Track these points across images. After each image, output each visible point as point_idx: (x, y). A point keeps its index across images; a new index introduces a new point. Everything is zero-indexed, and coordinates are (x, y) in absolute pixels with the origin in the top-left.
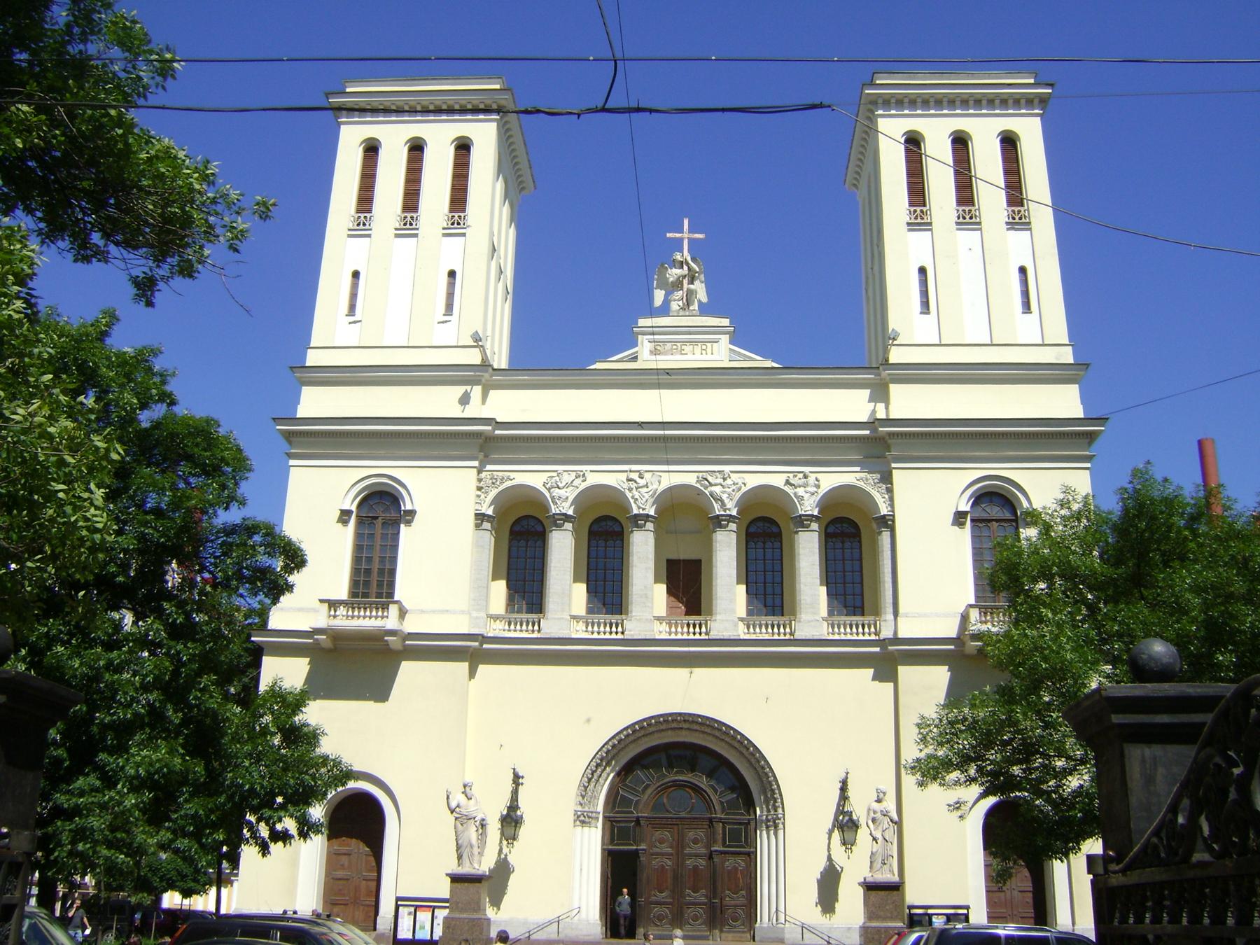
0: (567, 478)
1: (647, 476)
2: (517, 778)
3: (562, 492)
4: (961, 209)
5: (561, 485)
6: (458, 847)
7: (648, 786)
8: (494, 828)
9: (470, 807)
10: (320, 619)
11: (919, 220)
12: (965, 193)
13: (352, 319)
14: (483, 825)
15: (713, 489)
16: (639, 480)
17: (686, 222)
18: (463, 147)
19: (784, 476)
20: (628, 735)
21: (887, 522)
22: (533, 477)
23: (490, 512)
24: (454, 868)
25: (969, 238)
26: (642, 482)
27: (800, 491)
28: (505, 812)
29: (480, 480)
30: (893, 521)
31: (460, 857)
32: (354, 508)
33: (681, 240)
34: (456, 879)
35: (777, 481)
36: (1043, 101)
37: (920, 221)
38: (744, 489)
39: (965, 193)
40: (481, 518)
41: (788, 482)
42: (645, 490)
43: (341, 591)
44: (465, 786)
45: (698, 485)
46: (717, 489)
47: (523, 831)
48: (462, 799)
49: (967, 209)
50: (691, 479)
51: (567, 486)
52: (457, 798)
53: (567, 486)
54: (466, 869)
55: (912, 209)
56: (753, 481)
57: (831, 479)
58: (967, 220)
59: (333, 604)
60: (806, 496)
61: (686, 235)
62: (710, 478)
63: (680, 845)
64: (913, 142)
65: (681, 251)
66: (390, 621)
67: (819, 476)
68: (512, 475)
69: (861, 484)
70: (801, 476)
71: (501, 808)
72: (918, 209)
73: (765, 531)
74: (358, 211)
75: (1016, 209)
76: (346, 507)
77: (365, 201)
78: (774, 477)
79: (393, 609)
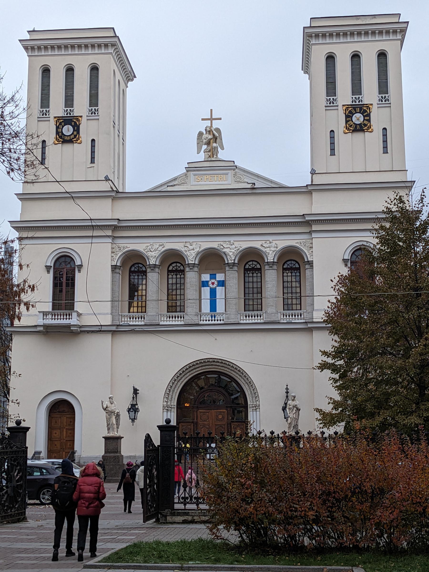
0: (156, 246)
2: (136, 391)
3: (153, 254)
4: (354, 97)
5: (152, 249)
6: (108, 425)
8: (125, 417)
9: (112, 408)
10: (40, 321)
14: (118, 416)
16: (190, 247)
19: (260, 243)
20: (187, 369)
21: (310, 263)
22: (139, 246)
23: (118, 264)
24: (106, 434)
26: (191, 247)
27: (268, 250)
28: (130, 407)
29: (112, 248)
31: (108, 429)
32: (52, 265)
34: (106, 438)
35: (257, 245)
38: (241, 249)
40: (114, 268)
43: (48, 307)
44: (110, 398)
47: (139, 415)
48: (109, 405)
50: (215, 245)
51: (155, 250)
52: (107, 403)
53: (155, 250)
54: (111, 434)
55: (328, 98)
56: (245, 245)
59: (45, 314)
60: (271, 252)
64: (331, 58)
66: (74, 321)
67: (276, 242)
68: (128, 245)
70: (268, 242)
71: (128, 405)
74: (42, 107)
76: (48, 264)
77: (45, 101)
78: (255, 243)
79: (74, 315)
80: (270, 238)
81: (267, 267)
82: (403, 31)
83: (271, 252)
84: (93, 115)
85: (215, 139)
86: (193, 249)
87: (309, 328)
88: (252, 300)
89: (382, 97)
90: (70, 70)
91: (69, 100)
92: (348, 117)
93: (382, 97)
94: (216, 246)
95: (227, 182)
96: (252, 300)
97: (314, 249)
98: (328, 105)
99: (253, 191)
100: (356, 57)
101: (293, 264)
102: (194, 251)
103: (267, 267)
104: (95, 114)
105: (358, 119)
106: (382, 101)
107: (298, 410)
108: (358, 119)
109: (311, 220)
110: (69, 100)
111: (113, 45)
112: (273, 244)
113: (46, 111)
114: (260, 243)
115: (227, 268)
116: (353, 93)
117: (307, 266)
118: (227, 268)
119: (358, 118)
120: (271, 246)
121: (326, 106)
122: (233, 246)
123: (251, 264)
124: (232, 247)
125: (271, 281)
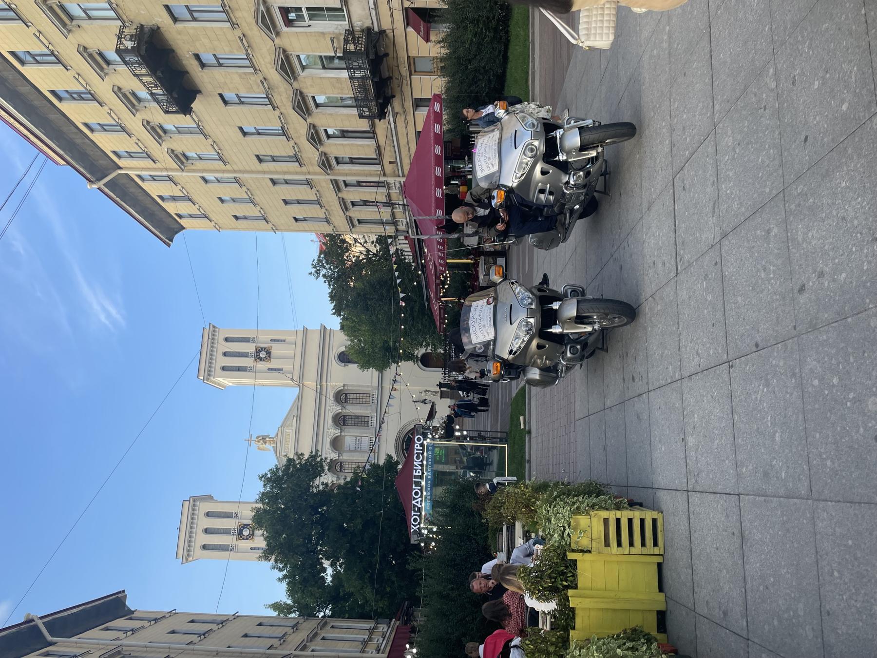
50: (329, 440)
80: (328, 408)
82: (214, 327)
85: (264, 439)
88: (361, 421)
91: (226, 532)
92: (261, 359)
95: (291, 431)
96: (361, 421)
99: (299, 416)
101: (342, 397)
105: (263, 354)
108: (263, 354)
110: (226, 532)
111: (194, 501)
116: (247, 356)
119: (263, 355)
120: (332, 408)
123: (340, 421)
124: (332, 431)
125: (352, 410)
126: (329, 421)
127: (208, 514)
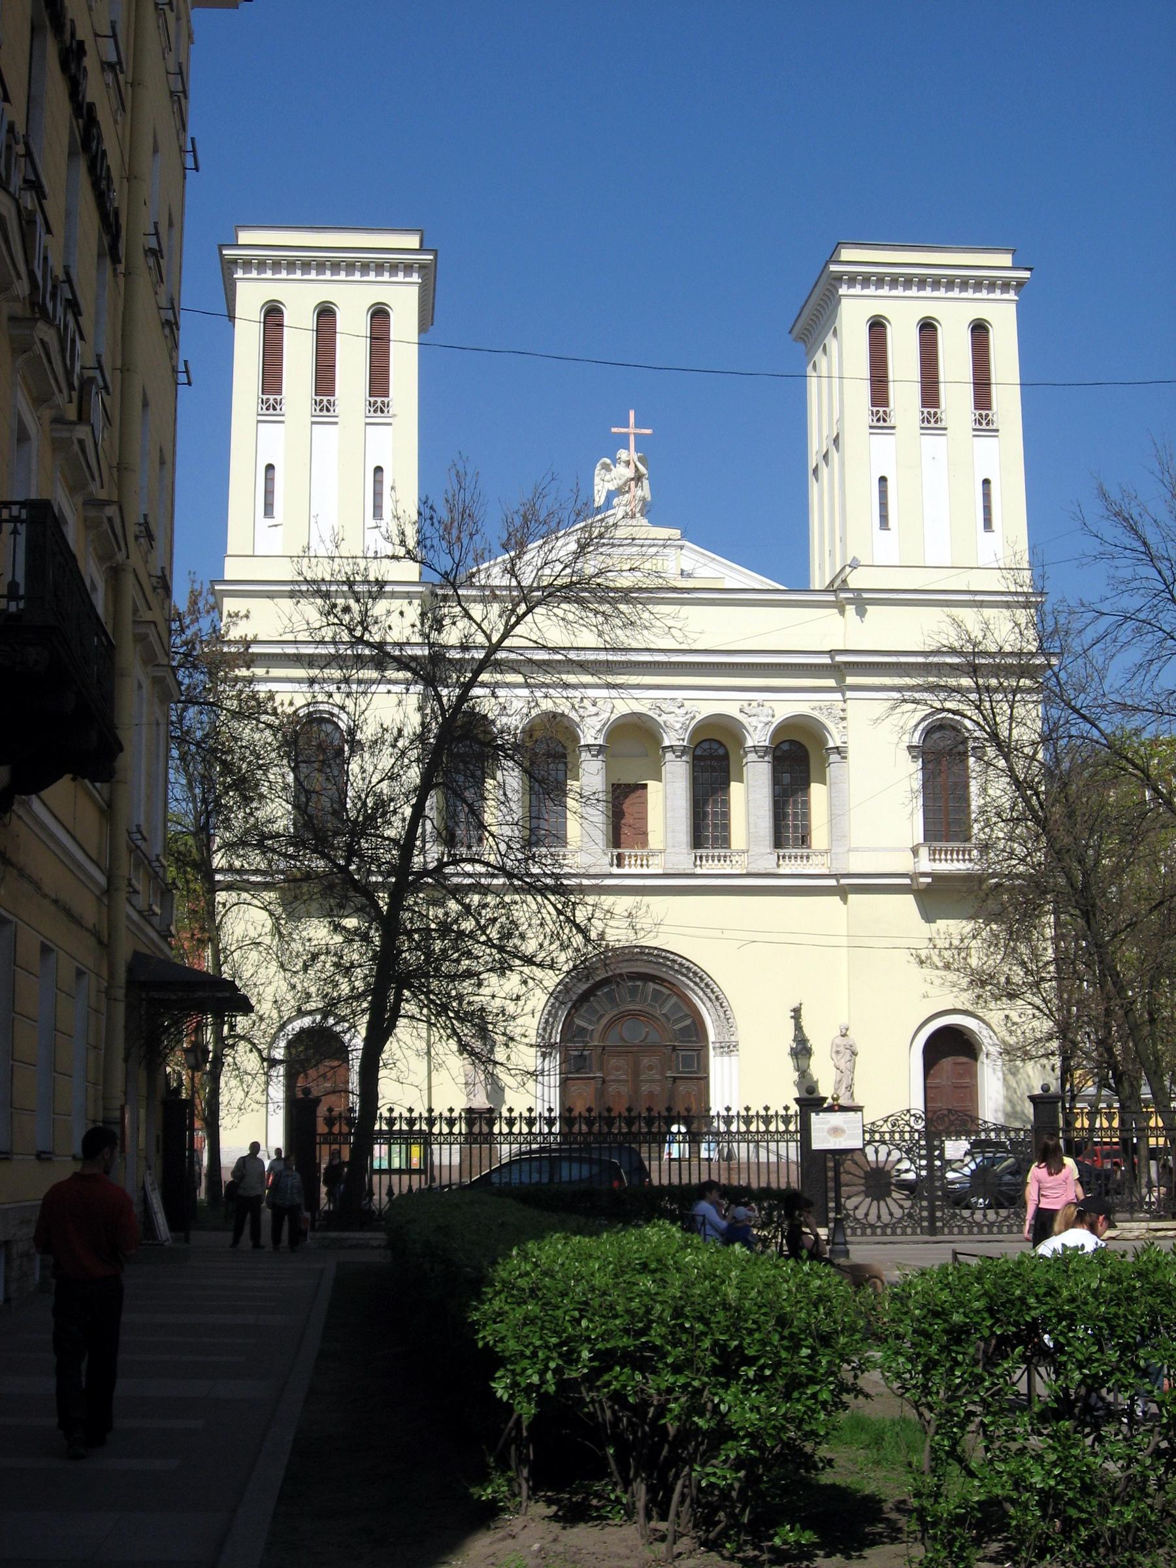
1: (600, 703)
4: (926, 410)
7: (602, 1016)
11: (881, 424)
12: (930, 394)
13: (271, 522)
15: (664, 717)
17: (632, 414)
18: (380, 314)
19: (738, 705)
25: (932, 443)
26: (593, 710)
30: (846, 752)
33: (627, 435)
36: (1020, 285)
37: (881, 422)
38: (699, 718)
39: (930, 394)
41: (741, 711)
42: (595, 718)
45: (650, 713)
46: (670, 719)
49: (932, 411)
57: (786, 707)
58: (932, 425)
61: (632, 430)
62: (664, 707)
63: (636, 1072)
64: (877, 327)
65: (627, 448)
69: (816, 714)
72: (881, 409)
73: (713, 757)
75: (984, 413)
77: (272, 378)
78: (728, 705)
81: (752, 757)
83: (760, 726)
84: (379, 413)
86: (597, 714)
87: (843, 887)
89: (981, 415)
90: (326, 313)
93: (981, 415)
94: (644, 710)
97: (849, 722)
98: (875, 424)
100: (928, 328)
102: (600, 718)
103: (752, 757)
104: (382, 411)
106: (980, 424)
107: (854, 1054)
109: (846, 663)
111: (423, 267)
112: (766, 710)
113: (275, 400)
114: (738, 705)
115: (669, 756)
117: (834, 757)
118: (669, 756)
120: (760, 714)
121: (871, 427)
122: (683, 711)
126: (707, 705)
127: (380, 314)
